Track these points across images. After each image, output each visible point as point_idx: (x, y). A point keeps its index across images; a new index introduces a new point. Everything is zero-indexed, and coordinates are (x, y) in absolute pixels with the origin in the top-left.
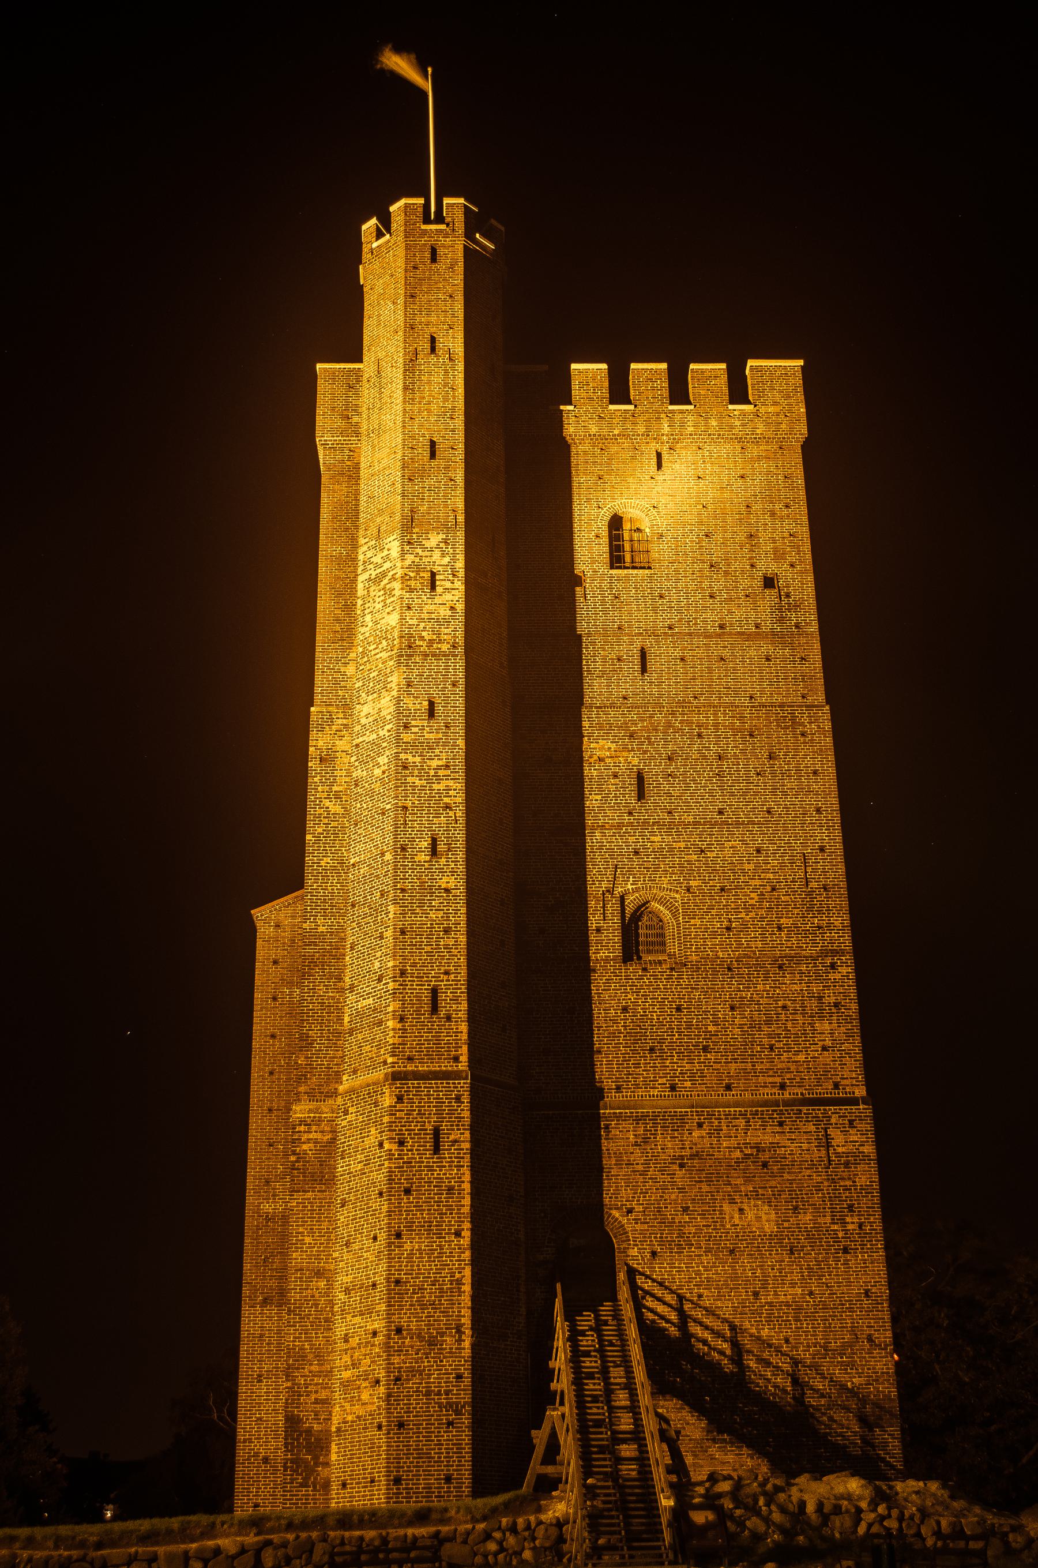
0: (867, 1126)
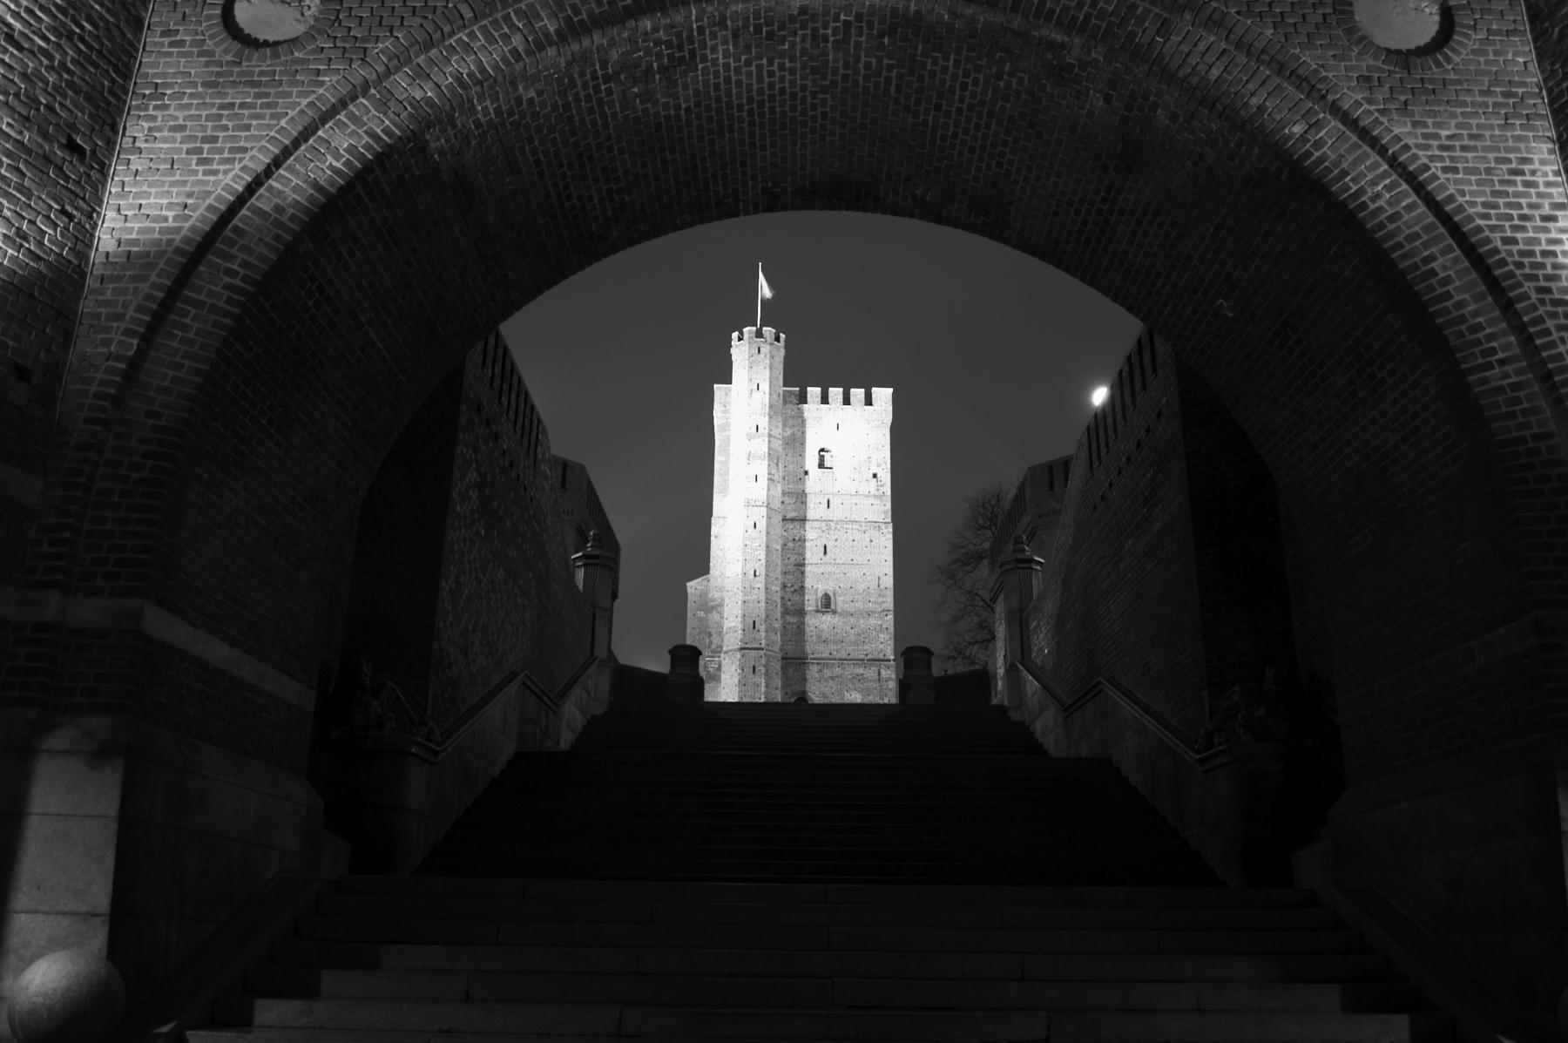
0: (893, 669)
